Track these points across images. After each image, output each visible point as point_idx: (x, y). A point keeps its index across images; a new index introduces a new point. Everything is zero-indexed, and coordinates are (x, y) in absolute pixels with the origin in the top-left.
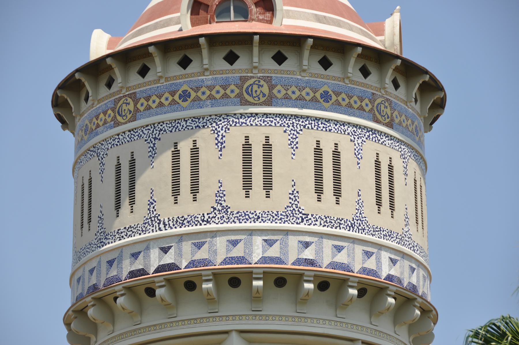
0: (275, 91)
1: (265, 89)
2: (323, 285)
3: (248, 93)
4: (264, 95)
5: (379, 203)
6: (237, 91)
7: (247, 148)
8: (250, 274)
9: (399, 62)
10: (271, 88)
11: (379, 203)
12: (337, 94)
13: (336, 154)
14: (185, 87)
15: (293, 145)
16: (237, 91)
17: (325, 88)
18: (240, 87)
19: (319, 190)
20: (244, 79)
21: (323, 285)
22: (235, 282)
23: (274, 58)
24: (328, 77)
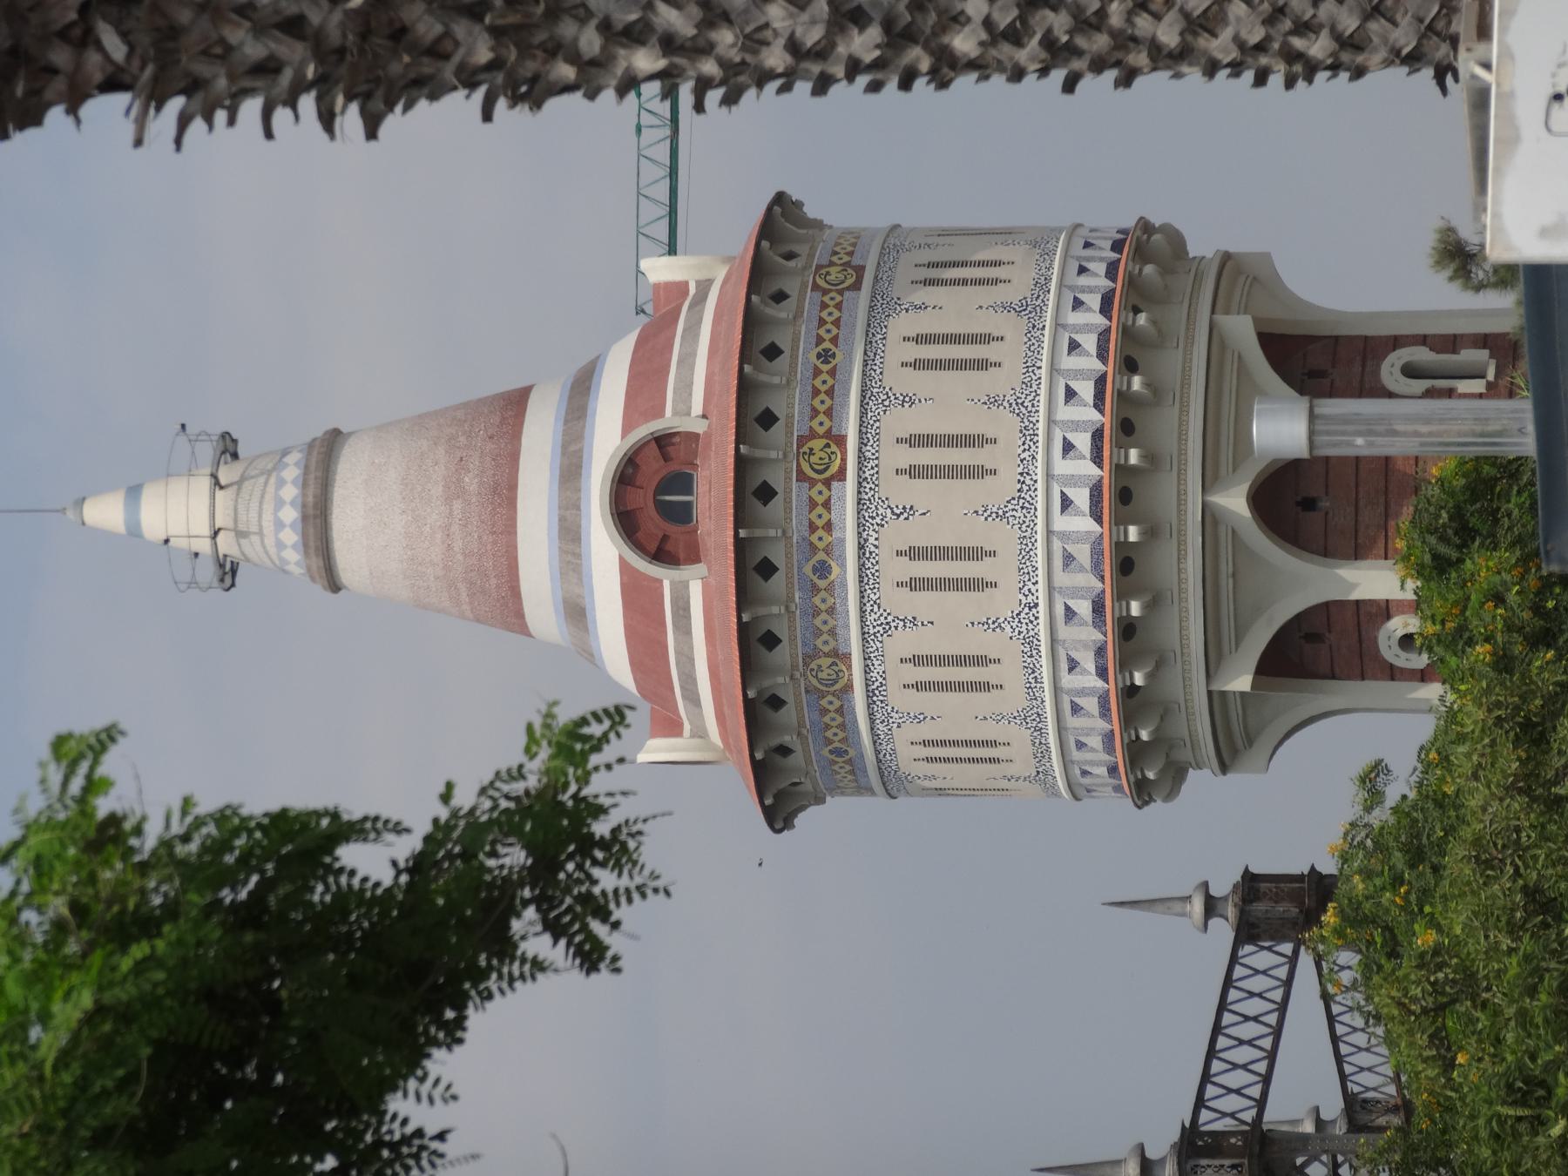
0: (821, 430)
1: (817, 444)
2: (1130, 365)
3: (825, 470)
4: (828, 445)
5: (996, 281)
6: (820, 486)
7: (914, 472)
8: (1121, 470)
9: (765, 244)
10: (813, 435)
11: (996, 281)
12: (820, 340)
13: (921, 339)
14: (808, 570)
15: (908, 400)
16: (820, 486)
17: (813, 357)
18: (812, 483)
19: (982, 365)
20: (802, 477)
21: (1130, 365)
22: (1124, 496)
23: (766, 429)
24: (795, 348)
